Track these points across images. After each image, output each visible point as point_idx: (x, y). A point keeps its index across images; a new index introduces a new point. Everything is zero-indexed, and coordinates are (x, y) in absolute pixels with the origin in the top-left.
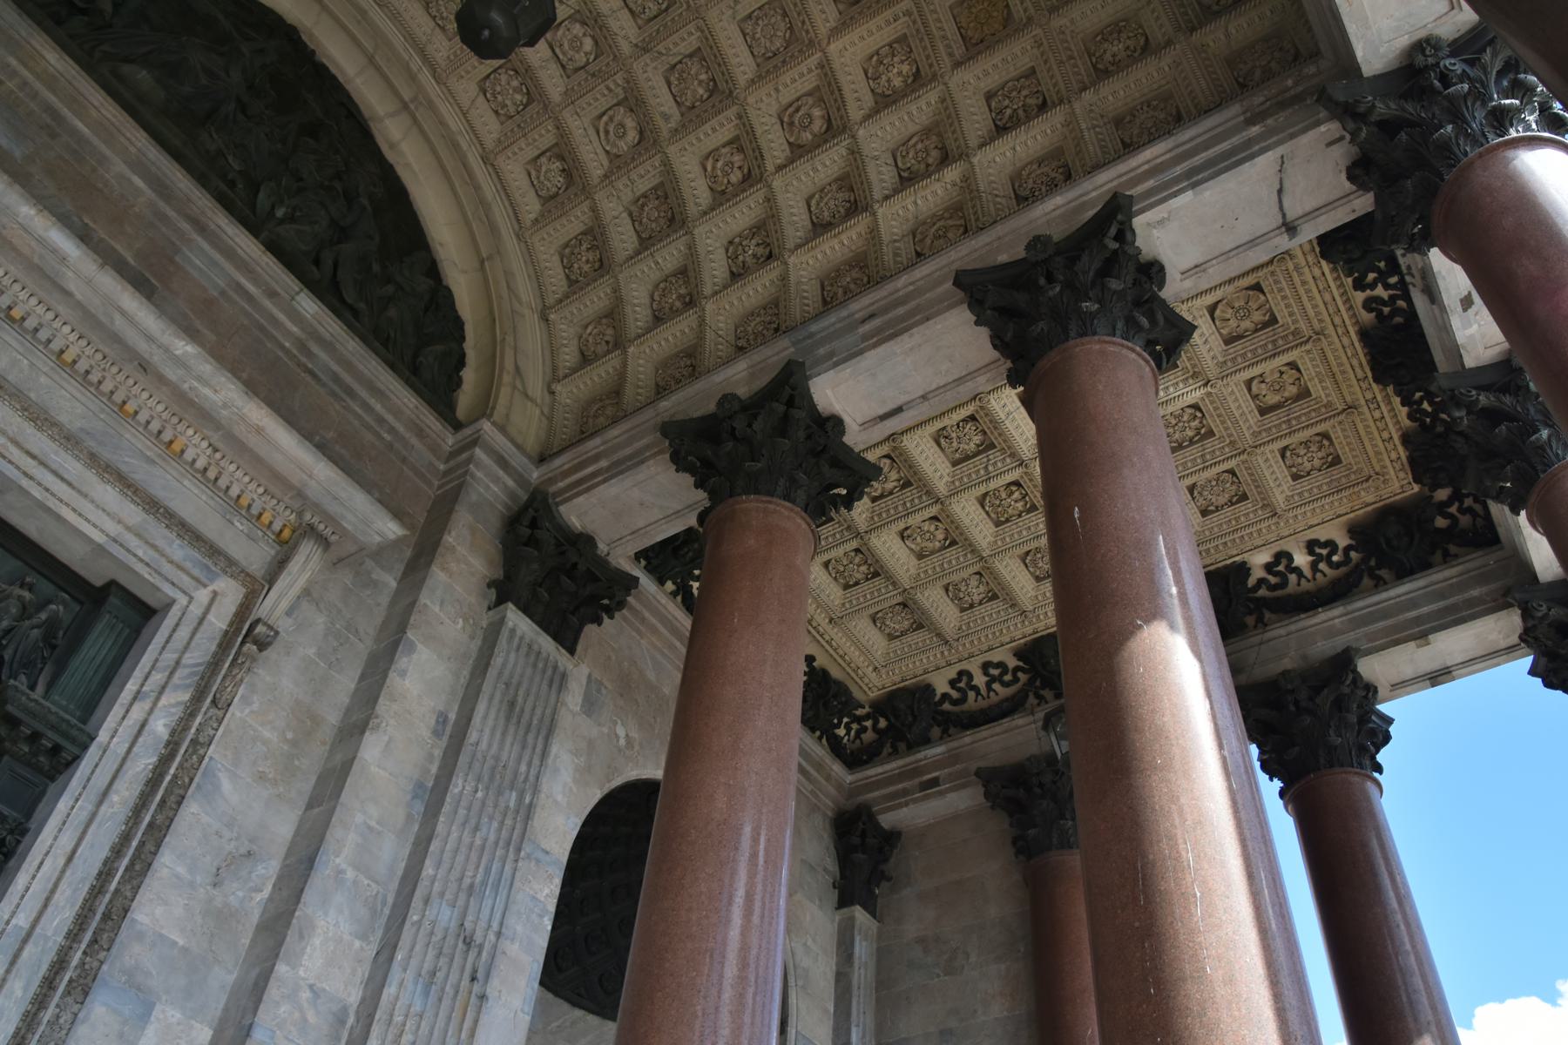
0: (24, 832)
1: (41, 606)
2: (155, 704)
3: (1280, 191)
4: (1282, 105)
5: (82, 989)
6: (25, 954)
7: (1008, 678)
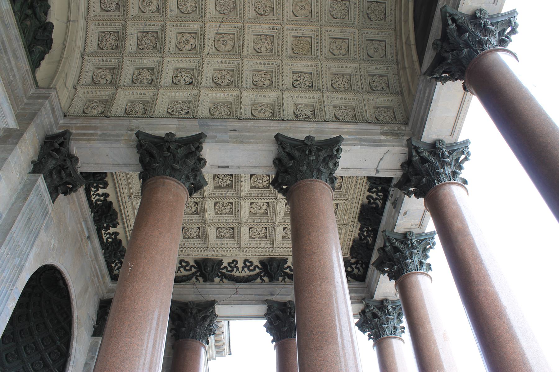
3: (381, 159)
4: (393, 134)
7: (188, 268)
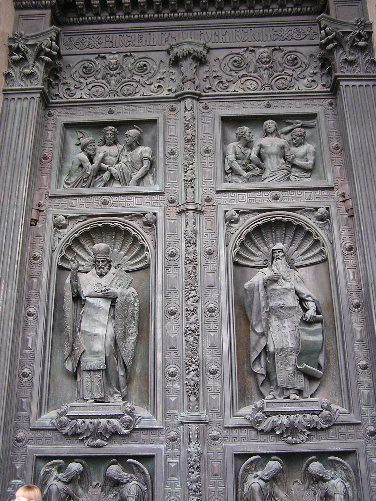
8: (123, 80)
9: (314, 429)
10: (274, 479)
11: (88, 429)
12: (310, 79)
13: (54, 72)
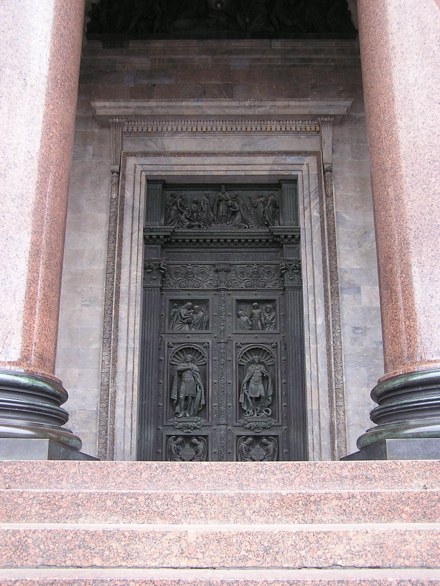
0: (300, 261)
1: (267, 200)
2: (310, 208)
5: (336, 293)
6: (316, 292)
8: (194, 279)
9: (265, 428)
10: (250, 444)
11: (185, 426)
12: (275, 282)
13: (163, 276)
